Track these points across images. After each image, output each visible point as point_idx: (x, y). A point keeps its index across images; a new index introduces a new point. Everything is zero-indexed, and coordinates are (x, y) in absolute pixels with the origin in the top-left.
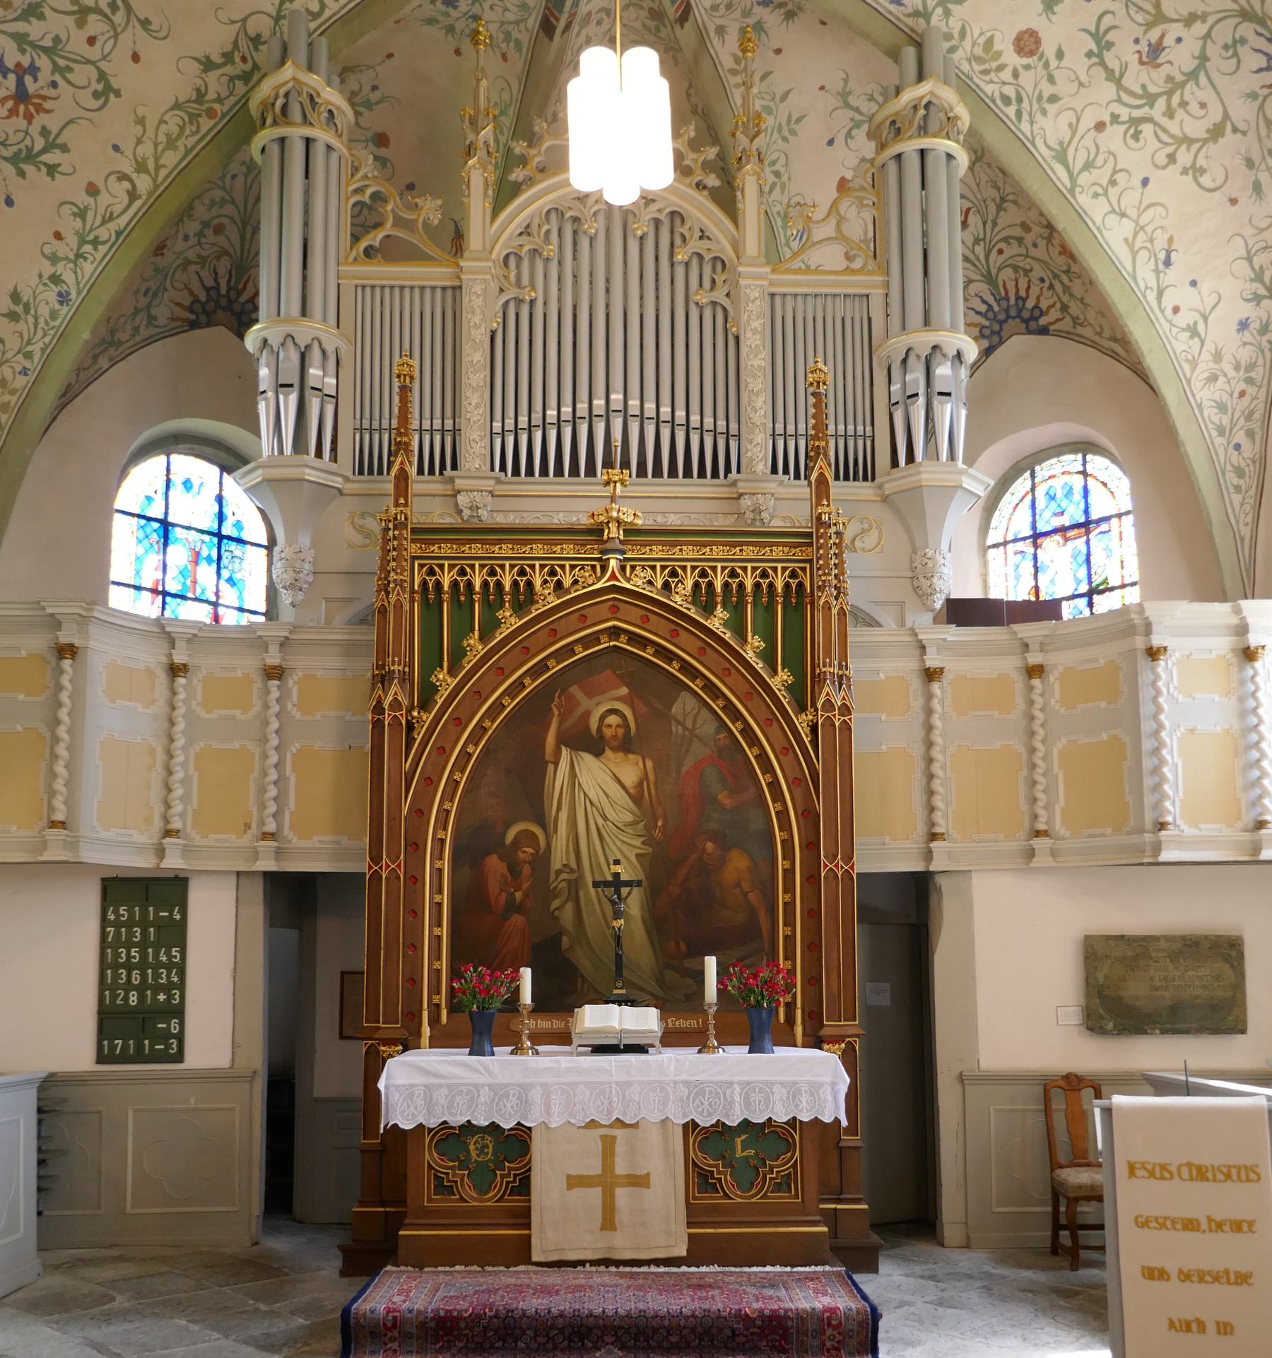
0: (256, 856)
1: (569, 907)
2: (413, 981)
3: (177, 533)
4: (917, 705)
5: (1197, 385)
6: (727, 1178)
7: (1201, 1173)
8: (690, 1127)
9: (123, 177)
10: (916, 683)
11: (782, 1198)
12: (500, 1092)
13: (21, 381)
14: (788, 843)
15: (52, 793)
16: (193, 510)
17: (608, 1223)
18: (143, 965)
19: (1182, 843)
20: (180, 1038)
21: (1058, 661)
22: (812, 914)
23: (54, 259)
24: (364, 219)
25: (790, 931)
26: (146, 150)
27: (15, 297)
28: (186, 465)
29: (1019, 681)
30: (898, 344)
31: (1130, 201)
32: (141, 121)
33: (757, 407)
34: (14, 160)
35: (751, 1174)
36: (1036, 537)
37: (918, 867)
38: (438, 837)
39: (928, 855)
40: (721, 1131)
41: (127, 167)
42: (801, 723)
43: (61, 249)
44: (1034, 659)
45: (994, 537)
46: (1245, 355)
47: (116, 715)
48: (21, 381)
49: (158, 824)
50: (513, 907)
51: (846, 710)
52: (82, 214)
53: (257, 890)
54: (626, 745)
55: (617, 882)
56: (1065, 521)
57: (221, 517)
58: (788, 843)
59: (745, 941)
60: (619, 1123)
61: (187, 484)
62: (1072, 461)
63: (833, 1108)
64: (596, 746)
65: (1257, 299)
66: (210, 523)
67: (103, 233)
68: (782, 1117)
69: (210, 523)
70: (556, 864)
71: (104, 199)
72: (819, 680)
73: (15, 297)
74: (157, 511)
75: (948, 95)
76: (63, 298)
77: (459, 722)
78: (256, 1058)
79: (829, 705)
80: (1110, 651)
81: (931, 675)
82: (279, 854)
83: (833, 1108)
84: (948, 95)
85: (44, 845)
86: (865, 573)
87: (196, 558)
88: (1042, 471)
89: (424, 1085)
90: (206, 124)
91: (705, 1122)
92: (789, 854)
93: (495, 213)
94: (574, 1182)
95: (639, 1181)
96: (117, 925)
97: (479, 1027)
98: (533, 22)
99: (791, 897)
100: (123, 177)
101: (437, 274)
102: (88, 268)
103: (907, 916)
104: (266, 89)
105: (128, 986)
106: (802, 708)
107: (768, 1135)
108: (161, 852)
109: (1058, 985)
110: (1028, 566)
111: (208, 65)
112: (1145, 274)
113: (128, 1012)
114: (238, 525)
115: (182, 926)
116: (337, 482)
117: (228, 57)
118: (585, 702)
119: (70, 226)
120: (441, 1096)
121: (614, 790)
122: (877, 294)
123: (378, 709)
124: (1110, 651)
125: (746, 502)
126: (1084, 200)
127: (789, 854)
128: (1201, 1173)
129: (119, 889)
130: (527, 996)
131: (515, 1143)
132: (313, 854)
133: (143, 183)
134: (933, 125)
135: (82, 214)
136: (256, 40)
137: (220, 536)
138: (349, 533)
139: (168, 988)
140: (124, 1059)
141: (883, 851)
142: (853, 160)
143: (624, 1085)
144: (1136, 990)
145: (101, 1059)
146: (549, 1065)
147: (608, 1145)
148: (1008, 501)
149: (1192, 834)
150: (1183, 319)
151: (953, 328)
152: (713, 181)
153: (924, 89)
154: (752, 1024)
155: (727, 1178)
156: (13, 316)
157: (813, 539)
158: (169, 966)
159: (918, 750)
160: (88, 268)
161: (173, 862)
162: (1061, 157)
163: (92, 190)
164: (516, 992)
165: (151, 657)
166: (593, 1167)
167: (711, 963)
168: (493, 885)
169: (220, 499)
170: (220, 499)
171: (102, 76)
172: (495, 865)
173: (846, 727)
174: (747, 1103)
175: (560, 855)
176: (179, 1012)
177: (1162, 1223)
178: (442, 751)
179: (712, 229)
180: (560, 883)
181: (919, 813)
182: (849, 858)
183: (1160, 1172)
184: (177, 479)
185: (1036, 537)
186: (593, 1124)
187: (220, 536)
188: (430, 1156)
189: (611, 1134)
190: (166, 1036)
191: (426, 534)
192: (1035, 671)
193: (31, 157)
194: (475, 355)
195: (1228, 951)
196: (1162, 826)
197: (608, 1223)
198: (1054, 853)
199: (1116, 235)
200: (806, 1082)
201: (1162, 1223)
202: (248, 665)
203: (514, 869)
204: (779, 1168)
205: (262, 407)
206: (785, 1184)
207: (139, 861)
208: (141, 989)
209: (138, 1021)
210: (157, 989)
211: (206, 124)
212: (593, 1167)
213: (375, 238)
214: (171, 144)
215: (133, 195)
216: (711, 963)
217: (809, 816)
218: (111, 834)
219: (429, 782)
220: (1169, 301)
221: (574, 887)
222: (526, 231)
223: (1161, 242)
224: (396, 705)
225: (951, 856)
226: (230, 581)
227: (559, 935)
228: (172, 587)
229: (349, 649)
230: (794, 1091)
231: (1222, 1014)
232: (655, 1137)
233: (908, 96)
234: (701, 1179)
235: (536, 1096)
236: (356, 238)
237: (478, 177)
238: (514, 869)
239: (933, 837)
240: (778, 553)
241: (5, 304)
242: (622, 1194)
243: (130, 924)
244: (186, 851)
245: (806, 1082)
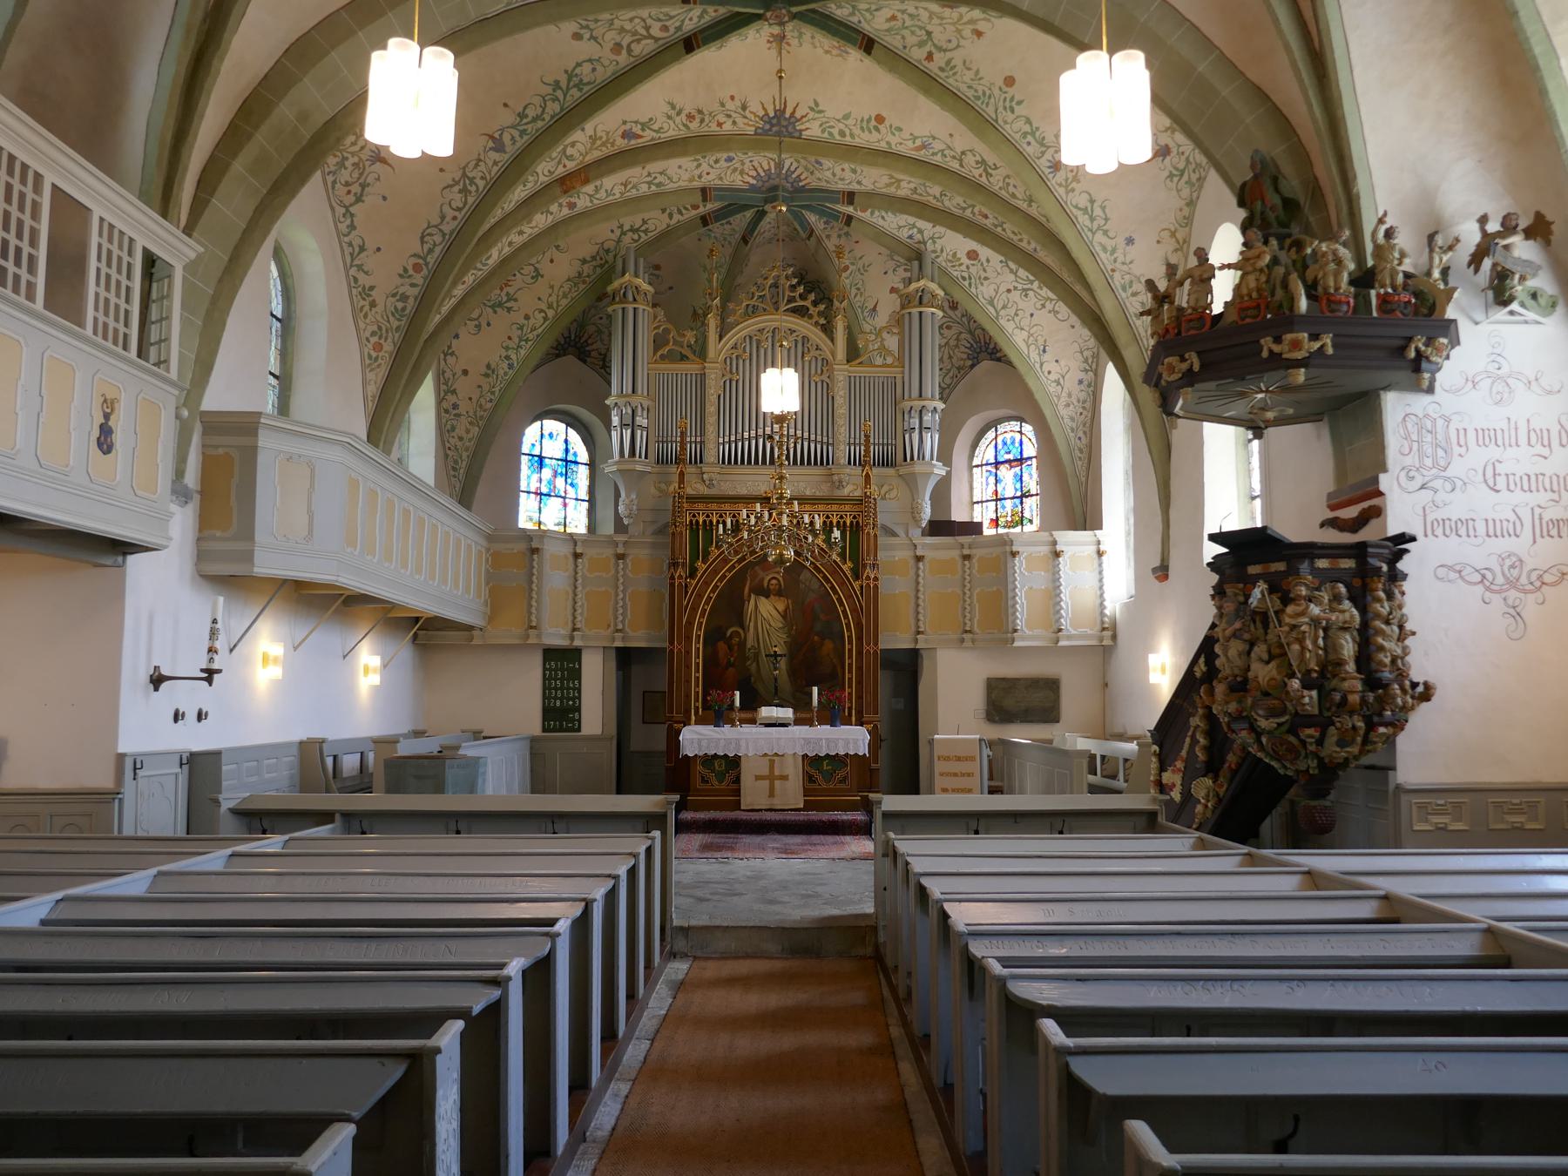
0: (614, 640)
2: (688, 696)
3: (547, 461)
4: (912, 573)
5: (1061, 408)
6: (819, 777)
7: (959, 759)
8: (805, 756)
9: (541, 311)
10: (912, 562)
11: (842, 786)
12: (728, 742)
13: (489, 405)
14: (850, 637)
15: (530, 613)
16: (553, 449)
17: (772, 794)
18: (562, 689)
19: (1023, 639)
21: (977, 553)
22: (859, 668)
23: (507, 348)
24: (658, 342)
25: (850, 676)
26: (553, 299)
27: (488, 366)
28: (552, 425)
29: (959, 560)
30: (907, 405)
31: (1025, 323)
32: (552, 287)
33: (842, 432)
34: (492, 307)
35: (829, 777)
36: (997, 464)
37: (911, 646)
38: (699, 633)
39: (916, 641)
40: (817, 759)
41: (544, 307)
42: (856, 585)
43: (511, 344)
44: (966, 552)
45: (976, 461)
46: (1082, 396)
47: (555, 578)
48: (489, 405)
49: (570, 626)
51: (876, 579)
52: (521, 328)
53: (613, 654)
54: (780, 593)
55: (776, 655)
56: (1011, 457)
57: (567, 451)
58: (850, 637)
59: (831, 680)
61: (551, 435)
62: (1015, 425)
63: (863, 750)
64: (765, 593)
65: (1086, 371)
66: (561, 455)
67: (530, 336)
69: (561, 455)
71: (532, 321)
72: (864, 566)
73: (488, 366)
74: (537, 452)
75: (933, 286)
76: (511, 366)
77: (707, 584)
79: (868, 578)
80: (998, 550)
81: (919, 559)
83: (863, 750)
84: (933, 286)
85: (528, 637)
86: (887, 512)
87: (555, 474)
88: (1001, 429)
89: (697, 739)
90: (582, 287)
92: (850, 642)
93: (721, 338)
94: (758, 778)
95: (784, 778)
96: (550, 670)
97: (717, 715)
98: (738, 236)
99: (851, 661)
100: (541, 311)
101: (692, 368)
102: (523, 352)
103: (907, 669)
104: (616, 284)
105: (556, 698)
106: (857, 577)
107: (837, 760)
108: (572, 638)
109: (976, 699)
110: (992, 480)
111: (584, 261)
112: (1034, 356)
114: (575, 454)
116: (648, 469)
117: (594, 258)
118: (761, 574)
119: (515, 334)
120: (704, 743)
121: (774, 613)
122: (899, 376)
123: (672, 578)
124: (998, 550)
125: (836, 478)
126: (1002, 322)
127: (850, 642)
128: (959, 759)
129: (551, 654)
130: (737, 703)
131: (734, 763)
132: (638, 641)
133: (551, 313)
134: (925, 300)
135: (521, 328)
136: (608, 251)
137: (566, 461)
138: (653, 490)
139: (573, 699)
141: (895, 638)
142: (897, 279)
144: (1009, 703)
146: (747, 730)
147: (772, 763)
148: (984, 442)
149: (1029, 632)
150: (1053, 377)
151: (933, 398)
152: (822, 321)
153: (922, 283)
154: (831, 715)
155: (819, 777)
156: (487, 375)
157: (863, 503)
159: (912, 594)
160: (523, 352)
161: (577, 643)
162: (991, 303)
163: (527, 317)
165: (566, 550)
166: (766, 772)
167: (815, 690)
168: (721, 654)
169: (566, 441)
170: (566, 441)
171: (536, 270)
172: (721, 645)
173: (876, 587)
176: (579, 710)
177: (948, 774)
178: (700, 596)
179: (822, 346)
181: (912, 622)
182: (876, 644)
183: (947, 759)
184: (546, 433)
185: (997, 464)
187: (566, 461)
188: (699, 768)
189: (773, 759)
191: (693, 499)
192: (967, 557)
193: (500, 305)
194: (711, 409)
195: (1052, 685)
196: (1016, 631)
197: (772, 794)
198: (973, 641)
199: (1019, 338)
200: (853, 739)
201: (948, 774)
202: (609, 552)
203: (730, 648)
204: (840, 774)
205: (614, 433)
206: (843, 780)
208: (561, 699)
209: (560, 712)
210: (569, 699)
211: (582, 287)
212: (766, 772)
213: (665, 350)
214: (565, 296)
215: (545, 319)
216: (815, 690)
217: (859, 625)
219: (694, 609)
220: (1046, 368)
221: (757, 655)
222: (735, 347)
223: (1041, 341)
224: (680, 577)
225: (926, 641)
226: (572, 485)
228: (545, 490)
229: (654, 546)
230: (847, 742)
231: (1049, 714)
232: (790, 760)
233: (914, 286)
234: (809, 778)
235: (743, 744)
236: (655, 351)
237: (712, 322)
238: (730, 648)
239: (919, 633)
240: (847, 508)
241: (484, 370)
242: (777, 783)
245: (853, 739)
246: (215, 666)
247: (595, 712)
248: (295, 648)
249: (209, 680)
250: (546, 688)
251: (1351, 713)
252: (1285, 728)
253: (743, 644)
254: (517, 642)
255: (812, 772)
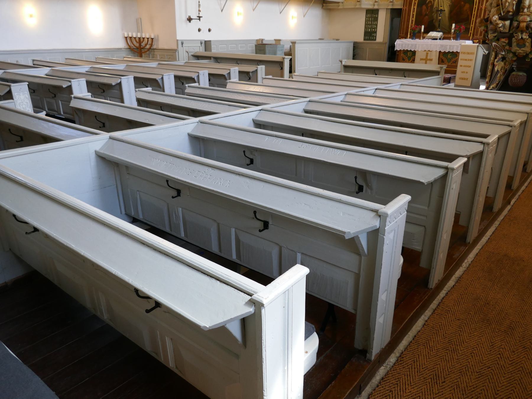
0: (388, 6)
1: (435, 15)
7: (468, 53)
8: (440, 52)
12: (412, 45)
20: (376, 37)
40: (445, 53)
50: (426, 15)
53: (389, 12)
60: (429, 51)
68: (455, 51)
70: (435, 7)
78: (387, 40)
82: (393, 5)
85: (356, 5)
89: (401, 44)
91: (442, 51)
97: (416, 35)
108: (374, 5)
113: (369, 32)
115: (377, 18)
120: (404, 45)
128: (468, 53)
130: (422, 30)
140: (367, 40)
143: (431, 45)
145: (364, 40)
147: (427, 54)
158: (375, 25)
164: (421, 29)
166: (424, 57)
167: (454, 25)
172: (424, 7)
174: (450, 48)
175: (435, 5)
176: (376, 32)
180: (434, 10)
183: (464, 53)
186: (425, 51)
189: (428, 52)
190: (374, 36)
203: (427, 8)
207: (370, 7)
208: (371, 28)
209: (370, 34)
210: (373, 28)
212: (424, 57)
218: (367, 3)
227: (433, 21)
235: (417, 46)
243: (370, 18)
244: (378, 5)
246: (200, 15)
247: (381, 34)
248: (254, 10)
249: (199, 19)
250: (366, 24)
251: (522, 32)
252: (496, 38)
253: (432, 6)
254: (353, 7)
255: (444, 58)
